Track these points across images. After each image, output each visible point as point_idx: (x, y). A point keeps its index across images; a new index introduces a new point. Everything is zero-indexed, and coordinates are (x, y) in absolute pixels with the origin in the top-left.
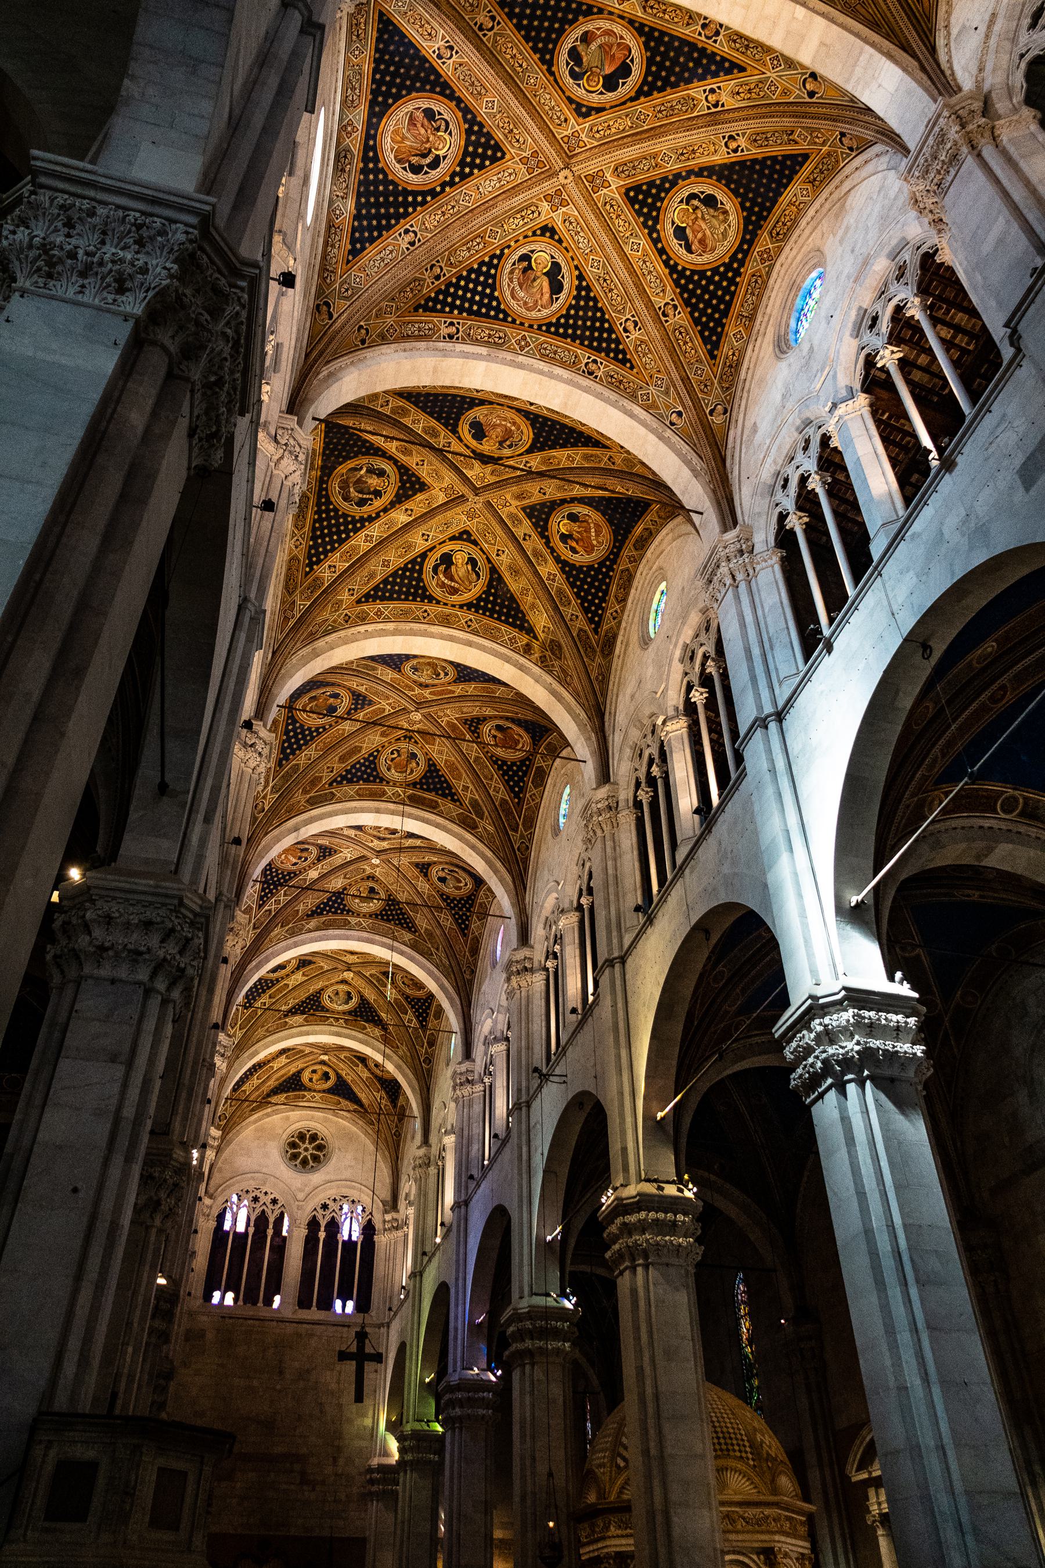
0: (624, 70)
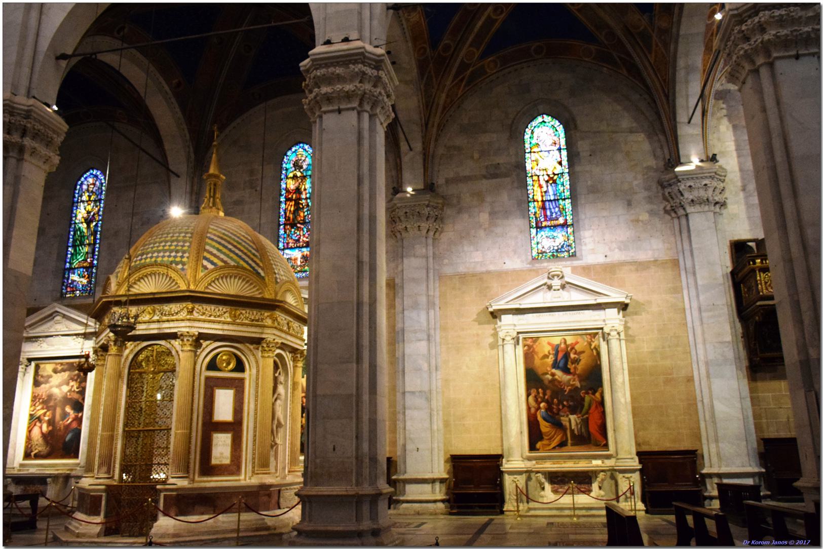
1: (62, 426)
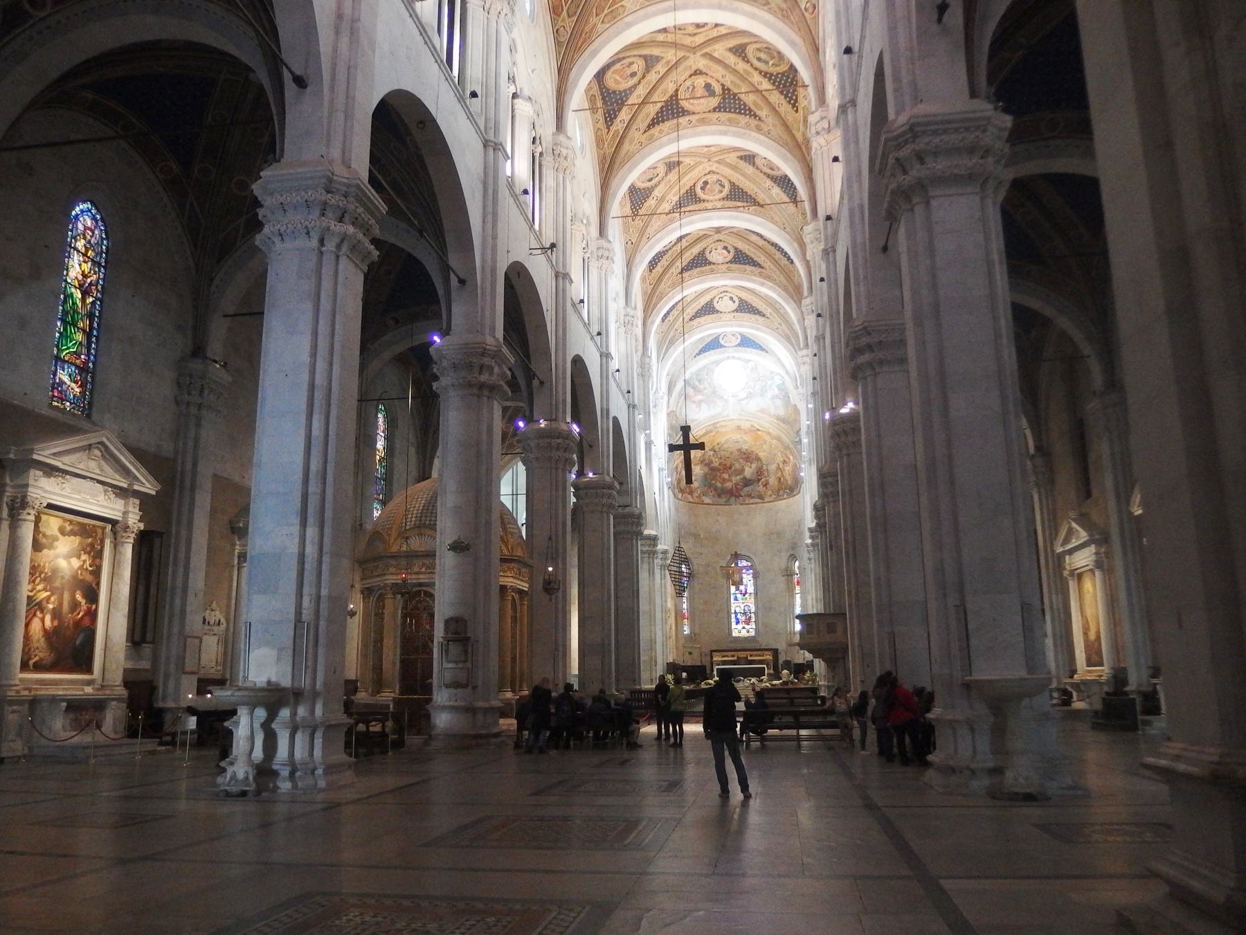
0: (703, 188)
1: (71, 622)
